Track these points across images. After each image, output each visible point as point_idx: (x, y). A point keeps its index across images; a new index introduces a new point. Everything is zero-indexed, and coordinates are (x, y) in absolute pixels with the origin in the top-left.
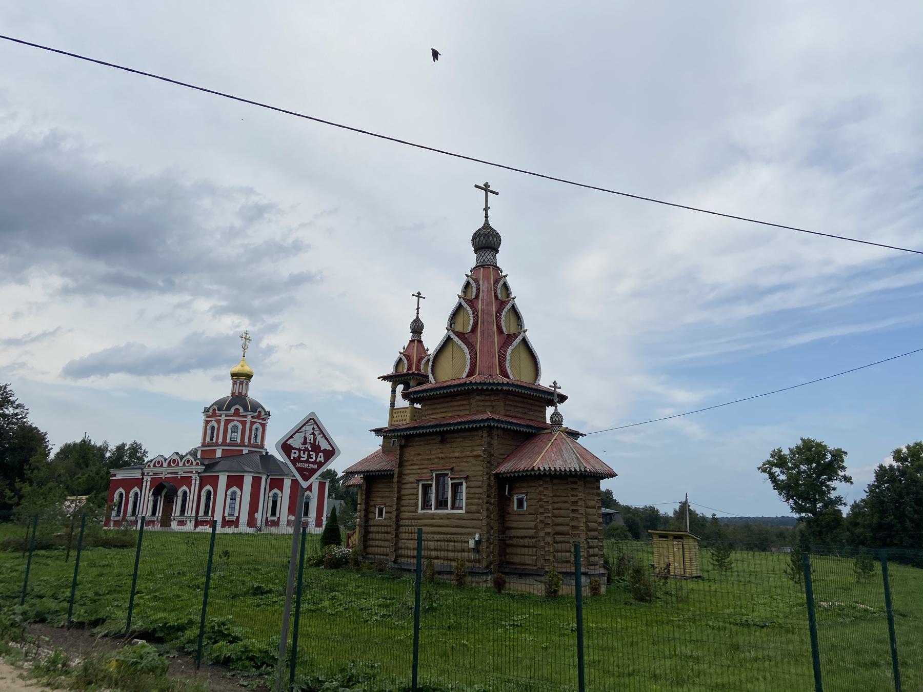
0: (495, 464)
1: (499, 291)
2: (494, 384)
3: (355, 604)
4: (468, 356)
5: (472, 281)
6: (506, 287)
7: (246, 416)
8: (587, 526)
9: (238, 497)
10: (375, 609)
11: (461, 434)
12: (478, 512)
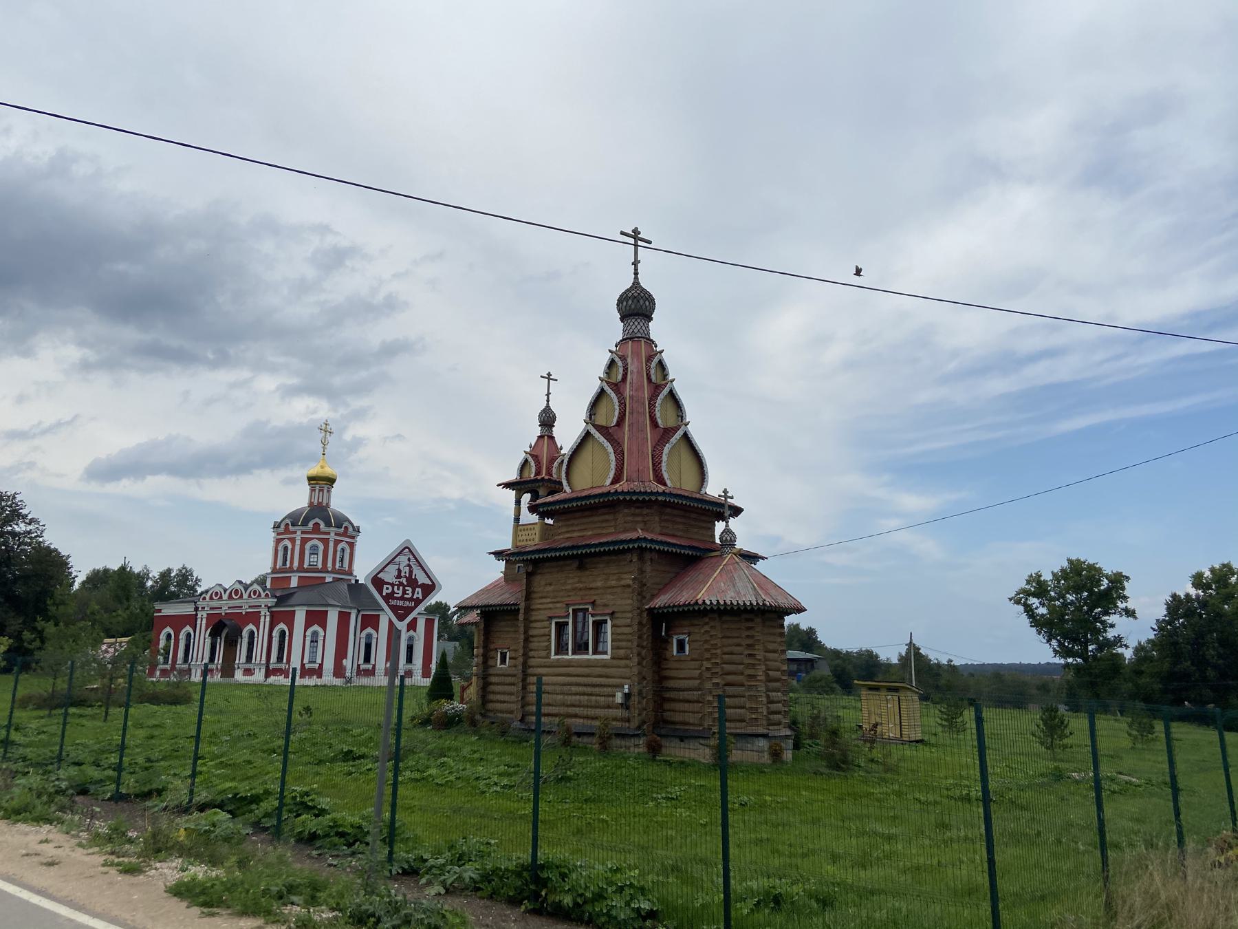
0: (648, 596)
1: (652, 371)
2: (646, 493)
3: (467, 773)
4: (612, 457)
5: (617, 359)
6: (661, 365)
7: (328, 533)
8: (767, 675)
9: (321, 639)
10: (495, 779)
11: (606, 558)
12: (627, 658)
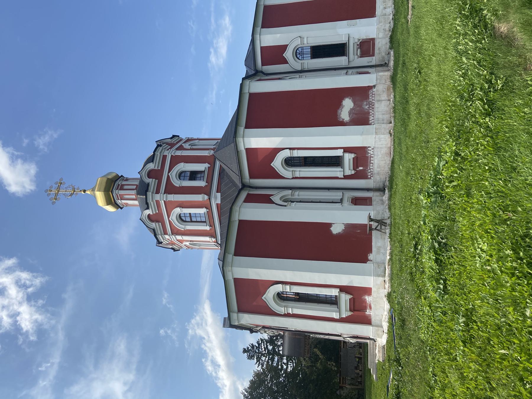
7: (158, 202)
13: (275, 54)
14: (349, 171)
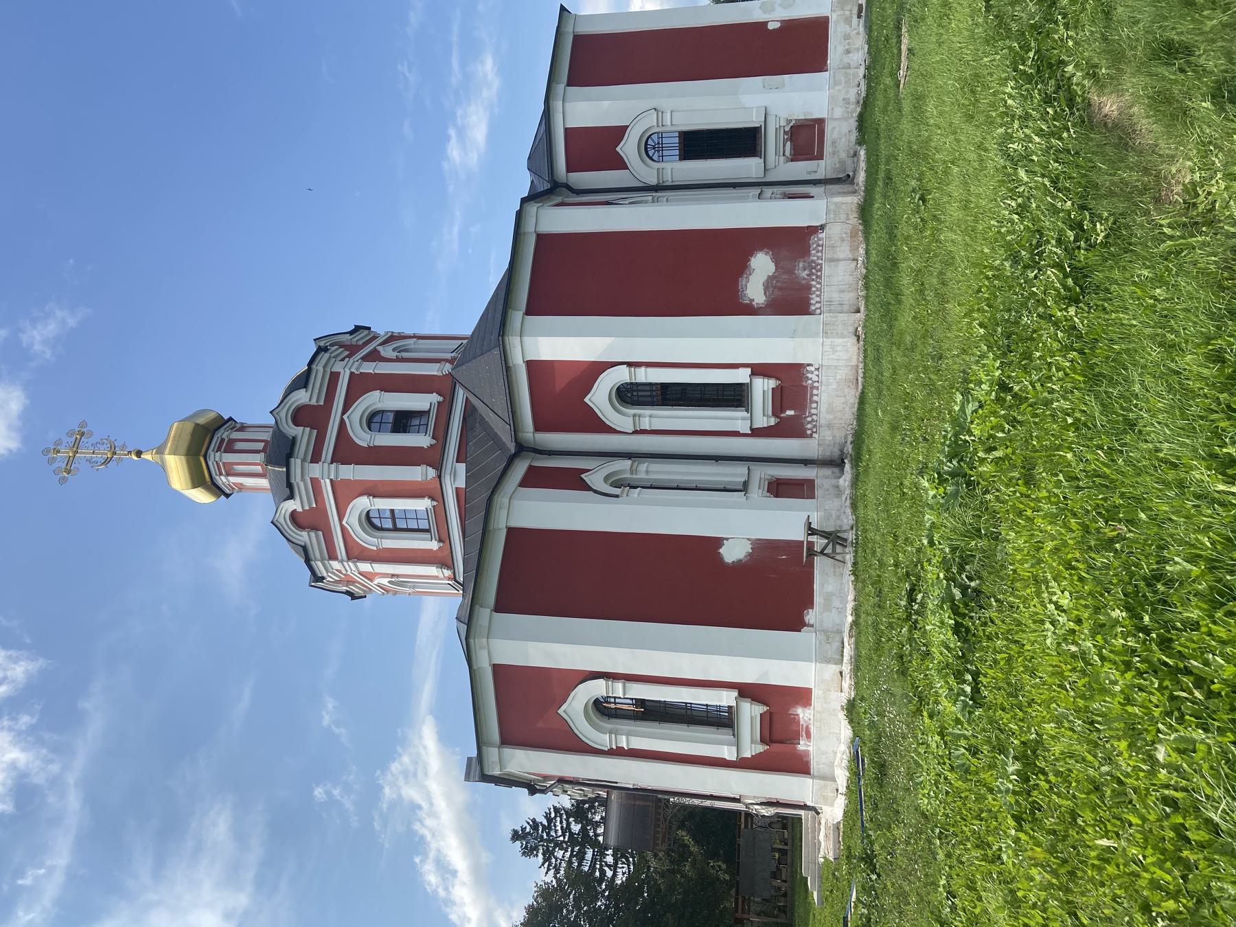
7: (315, 483)
13: (597, 147)
14: (763, 420)
